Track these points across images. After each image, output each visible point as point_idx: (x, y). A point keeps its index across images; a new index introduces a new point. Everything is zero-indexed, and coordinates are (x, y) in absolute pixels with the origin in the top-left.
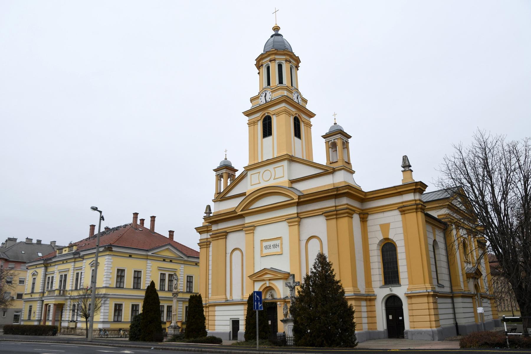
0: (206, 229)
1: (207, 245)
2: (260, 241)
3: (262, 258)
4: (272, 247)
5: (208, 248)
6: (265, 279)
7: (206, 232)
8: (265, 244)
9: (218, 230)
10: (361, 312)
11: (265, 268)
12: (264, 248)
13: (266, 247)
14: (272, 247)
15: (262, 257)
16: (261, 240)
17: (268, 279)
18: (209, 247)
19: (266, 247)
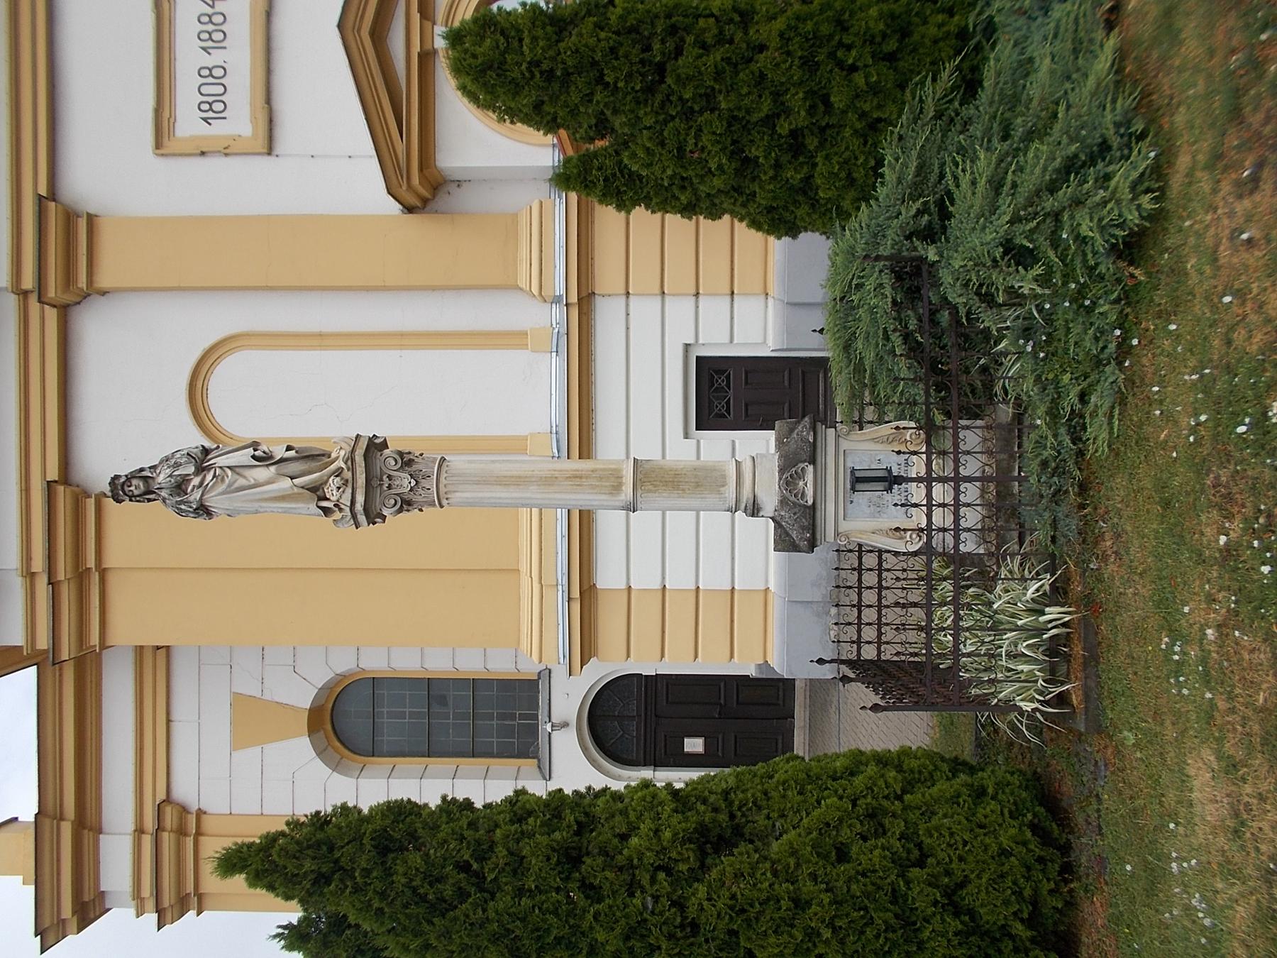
0: (67, 829)
1: (181, 832)
2: (162, 163)
3: (279, 147)
4: (216, 58)
5: (208, 824)
6: (416, 49)
7: (87, 836)
8: (188, 123)
9: (30, 576)
10: (697, 294)
11: (341, 26)
12: (218, 128)
13: (212, 109)
14: (216, 58)
15: (277, 150)
16: (158, 145)
17: (416, 17)
18: (200, 813)
19: (212, 109)
